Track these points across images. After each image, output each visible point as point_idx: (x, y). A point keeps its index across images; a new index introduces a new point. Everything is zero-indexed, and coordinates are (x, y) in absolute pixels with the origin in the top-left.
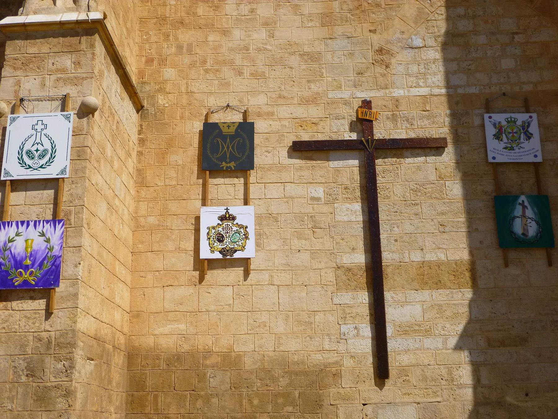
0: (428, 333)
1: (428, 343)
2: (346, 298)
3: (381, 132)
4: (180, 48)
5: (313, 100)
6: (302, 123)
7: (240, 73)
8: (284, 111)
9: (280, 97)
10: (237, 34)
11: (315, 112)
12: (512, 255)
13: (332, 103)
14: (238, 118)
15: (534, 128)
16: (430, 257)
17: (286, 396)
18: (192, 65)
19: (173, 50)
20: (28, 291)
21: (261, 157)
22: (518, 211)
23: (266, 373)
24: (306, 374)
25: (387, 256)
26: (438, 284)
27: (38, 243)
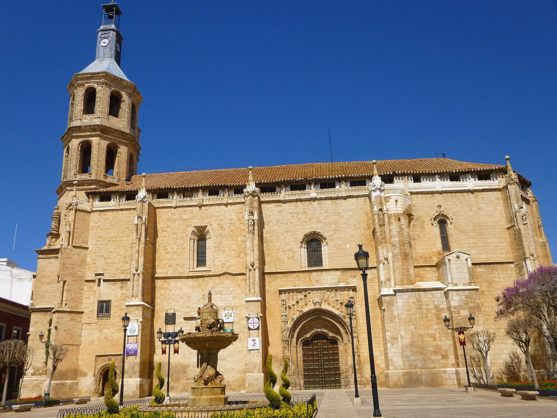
5: (189, 307)
6: (186, 313)
8: (182, 310)
10: (173, 291)
11: (188, 310)
14: (172, 312)
15: (233, 314)
17: (180, 371)
20: (132, 355)
21: (177, 321)
23: (176, 366)
27: (133, 347)
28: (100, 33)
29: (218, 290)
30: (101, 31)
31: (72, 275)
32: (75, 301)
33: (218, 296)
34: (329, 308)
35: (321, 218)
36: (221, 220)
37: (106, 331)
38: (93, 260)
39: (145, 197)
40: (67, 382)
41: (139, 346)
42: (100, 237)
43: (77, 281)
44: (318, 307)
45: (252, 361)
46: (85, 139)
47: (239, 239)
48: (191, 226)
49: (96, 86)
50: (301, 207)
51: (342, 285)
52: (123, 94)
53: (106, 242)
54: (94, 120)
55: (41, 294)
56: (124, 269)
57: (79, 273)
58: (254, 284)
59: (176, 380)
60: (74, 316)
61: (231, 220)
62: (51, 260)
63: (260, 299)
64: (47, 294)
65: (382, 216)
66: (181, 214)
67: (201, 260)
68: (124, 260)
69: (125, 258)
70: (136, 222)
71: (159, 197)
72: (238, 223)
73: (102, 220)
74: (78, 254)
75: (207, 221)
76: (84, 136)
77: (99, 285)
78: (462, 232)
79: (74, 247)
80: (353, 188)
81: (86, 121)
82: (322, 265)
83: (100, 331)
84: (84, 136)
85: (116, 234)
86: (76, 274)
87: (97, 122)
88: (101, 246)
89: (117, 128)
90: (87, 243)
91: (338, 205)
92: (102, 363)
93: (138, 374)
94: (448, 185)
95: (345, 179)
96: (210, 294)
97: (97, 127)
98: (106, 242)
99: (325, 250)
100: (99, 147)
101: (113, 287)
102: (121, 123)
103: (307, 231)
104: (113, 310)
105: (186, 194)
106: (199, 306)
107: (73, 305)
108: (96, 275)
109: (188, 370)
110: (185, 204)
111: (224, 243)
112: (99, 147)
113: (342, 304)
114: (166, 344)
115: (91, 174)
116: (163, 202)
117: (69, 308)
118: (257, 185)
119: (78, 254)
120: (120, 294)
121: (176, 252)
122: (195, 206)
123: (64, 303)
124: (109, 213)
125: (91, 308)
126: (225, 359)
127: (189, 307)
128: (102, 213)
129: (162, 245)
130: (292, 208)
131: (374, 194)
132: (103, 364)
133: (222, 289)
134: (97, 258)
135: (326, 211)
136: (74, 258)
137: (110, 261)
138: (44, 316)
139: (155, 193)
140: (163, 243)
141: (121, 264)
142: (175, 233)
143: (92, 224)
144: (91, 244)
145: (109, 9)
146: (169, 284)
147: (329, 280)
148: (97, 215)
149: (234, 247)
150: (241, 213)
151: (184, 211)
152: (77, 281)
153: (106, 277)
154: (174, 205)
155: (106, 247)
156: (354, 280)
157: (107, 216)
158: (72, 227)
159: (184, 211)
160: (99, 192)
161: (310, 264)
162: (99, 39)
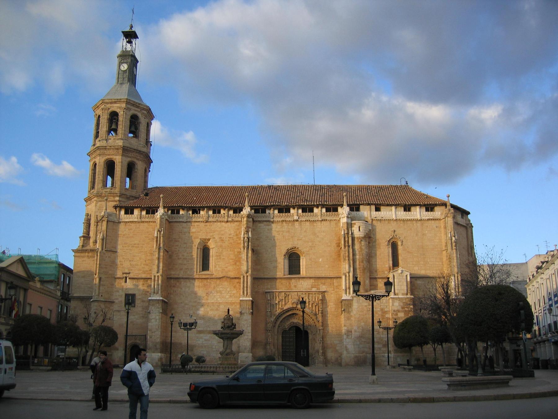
5: (195, 302)
10: (183, 289)
29: (218, 289)
33: (219, 294)
35: (301, 236)
36: (223, 235)
45: (244, 344)
47: (236, 250)
49: (118, 110)
50: (286, 227)
51: (314, 289)
54: (117, 141)
56: (145, 270)
57: (110, 272)
58: (247, 287)
61: (230, 235)
62: (84, 259)
63: (251, 299)
67: (205, 266)
68: (144, 262)
72: (235, 237)
73: (127, 230)
75: (211, 234)
76: (109, 155)
77: (126, 282)
78: (408, 252)
82: (300, 273)
89: (135, 148)
93: (159, 350)
94: (401, 214)
96: (229, 310)
99: (303, 262)
103: (290, 246)
104: (138, 302)
108: (123, 273)
111: (224, 253)
118: (252, 208)
119: (109, 257)
121: (186, 259)
124: (133, 225)
125: (120, 299)
127: (195, 302)
130: (279, 227)
133: (221, 289)
135: (305, 231)
137: (134, 263)
143: (120, 233)
147: (303, 286)
149: (232, 256)
150: (238, 229)
153: (131, 275)
156: (324, 287)
161: (291, 272)
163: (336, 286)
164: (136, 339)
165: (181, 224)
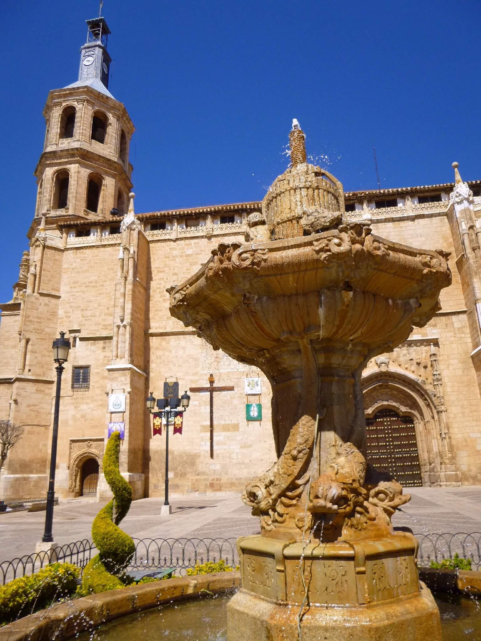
0: (225, 444)
1: (225, 447)
2: (203, 434)
3: (215, 385)
4: (157, 357)
5: (196, 374)
6: (192, 381)
7: (175, 365)
9: (186, 373)
10: (174, 352)
11: (196, 378)
12: (250, 422)
13: (202, 375)
14: (174, 380)
15: (259, 383)
16: (227, 423)
18: (161, 363)
19: (155, 358)
22: (252, 409)
23: (181, 456)
24: (191, 456)
25: (215, 422)
26: (229, 430)
27: (118, 428)
28: (83, 51)
30: (85, 48)
31: (39, 331)
32: (43, 367)
34: (401, 371)
37: (84, 407)
38: (66, 312)
39: (133, 223)
40: (31, 476)
41: (127, 427)
42: (75, 282)
43: (45, 339)
44: (384, 369)
46: (61, 167)
48: (196, 263)
49: (75, 104)
52: (110, 116)
53: (83, 288)
55: (5, 361)
56: (107, 323)
57: (47, 330)
59: (181, 475)
60: (40, 385)
64: (12, 361)
65: (474, 237)
66: (183, 248)
68: (106, 311)
69: (108, 308)
70: (121, 255)
71: (154, 228)
74: (45, 305)
76: (60, 164)
79: (42, 294)
80: (423, 205)
81: (63, 146)
83: (75, 407)
84: (60, 164)
85: (96, 278)
86: (43, 331)
87: (76, 145)
88: (77, 294)
90: (59, 291)
91: (404, 229)
92: (79, 451)
95: (412, 194)
97: (76, 151)
98: (83, 288)
100: (79, 176)
101: (93, 348)
102: (108, 149)
104: (93, 379)
105: (189, 222)
106: (211, 372)
107: (39, 371)
109: (198, 461)
110: (188, 236)
112: (79, 176)
113: (418, 364)
114: (161, 417)
115: (68, 209)
116: (159, 234)
117: (33, 375)
119: (45, 305)
120: (101, 357)
122: (202, 237)
123: (27, 368)
124: (87, 251)
126: (251, 446)
127: (196, 374)
128: (78, 251)
129: (158, 291)
131: (458, 208)
132: (80, 453)
134: (71, 310)
136: (41, 308)
137: (89, 313)
138: (8, 389)
139: (148, 223)
140: (160, 288)
141: (103, 317)
142: (175, 274)
143: (65, 266)
144: (64, 291)
145: (94, 25)
146: (168, 343)
148: (72, 255)
151: (188, 245)
152: (45, 339)
153: (83, 334)
154: (173, 237)
155: (84, 296)
156: (435, 331)
157: (85, 255)
158: (38, 269)
159: (188, 245)
160: (74, 225)
162: (82, 57)
163: (459, 329)
164: (89, 447)
165: (168, 243)
